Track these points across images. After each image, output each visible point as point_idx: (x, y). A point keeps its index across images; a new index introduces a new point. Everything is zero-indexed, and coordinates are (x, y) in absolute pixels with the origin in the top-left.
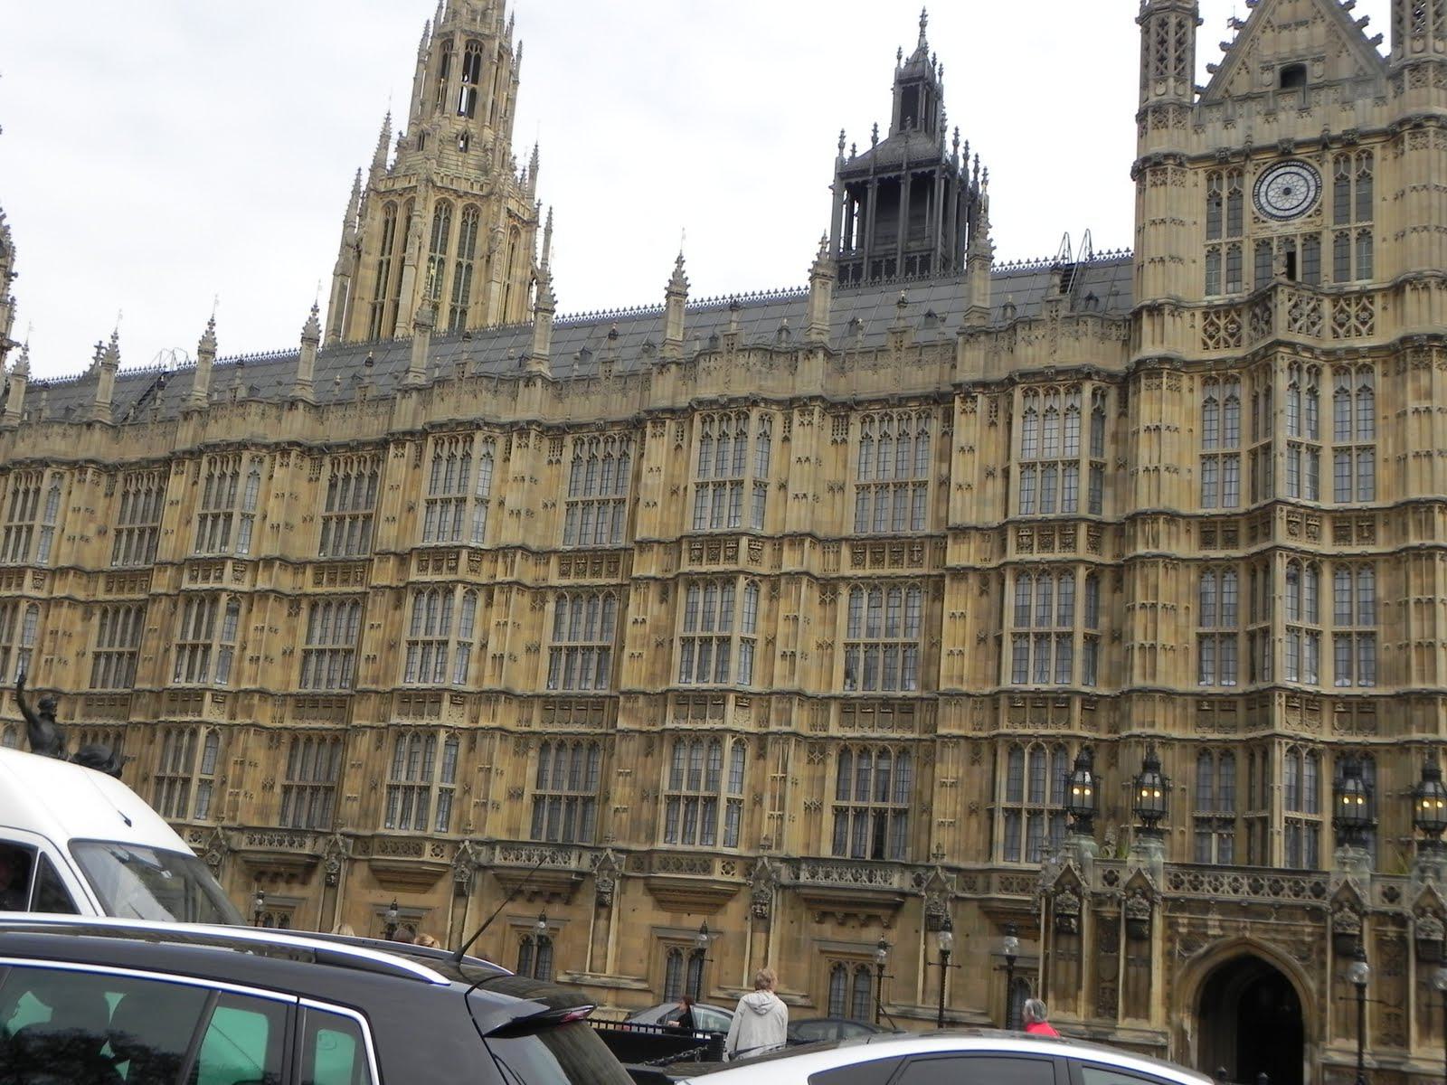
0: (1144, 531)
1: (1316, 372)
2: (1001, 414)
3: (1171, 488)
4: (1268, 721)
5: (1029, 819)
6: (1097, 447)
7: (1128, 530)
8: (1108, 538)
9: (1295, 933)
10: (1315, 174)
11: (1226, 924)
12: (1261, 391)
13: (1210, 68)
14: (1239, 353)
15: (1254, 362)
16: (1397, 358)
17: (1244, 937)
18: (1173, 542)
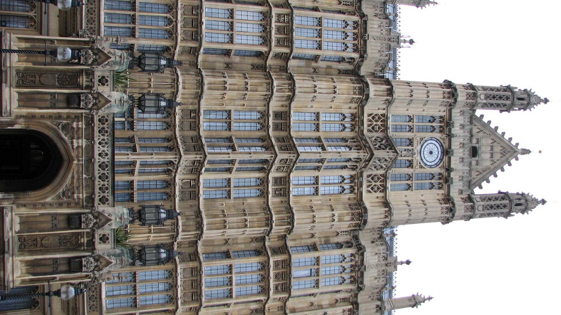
1: (354, 168)
2: (345, 8)
3: (305, 98)
4: (187, 151)
7: (284, 75)
8: (279, 62)
9: (78, 188)
10: (437, 165)
11: (80, 150)
12: (348, 143)
13: (482, 116)
14: (365, 132)
15: (362, 139)
16: (356, 205)
17: (73, 160)
18: (278, 99)
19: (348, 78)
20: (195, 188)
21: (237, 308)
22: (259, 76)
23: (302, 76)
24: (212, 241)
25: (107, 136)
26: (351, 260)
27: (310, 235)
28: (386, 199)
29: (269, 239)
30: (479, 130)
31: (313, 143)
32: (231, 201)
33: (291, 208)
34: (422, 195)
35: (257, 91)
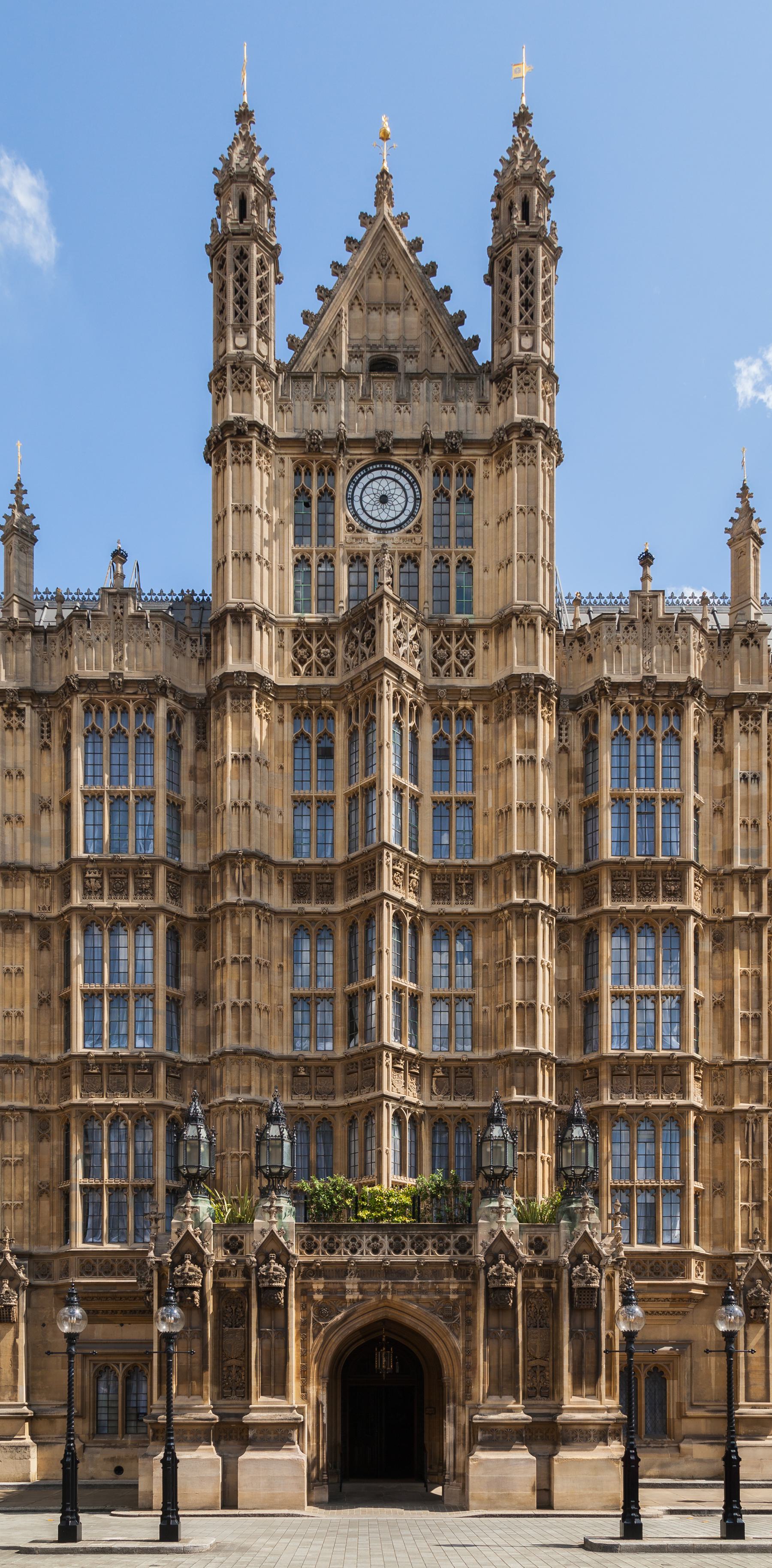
0: (234, 878)
3: (261, 830)
6: (174, 782)
14: (334, 681)
18: (265, 892)
19: (215, 726)
20: (449, 1068)
21: (707, 980)
22: (219, 934)
24: (559, 1032)
26: (628, 714)
27: (563, 818)
29: (564, 910)
30: (329, 349)
32: (479, 992)
33: (501, 861)
34: (486, 524)
35: (250, 939)
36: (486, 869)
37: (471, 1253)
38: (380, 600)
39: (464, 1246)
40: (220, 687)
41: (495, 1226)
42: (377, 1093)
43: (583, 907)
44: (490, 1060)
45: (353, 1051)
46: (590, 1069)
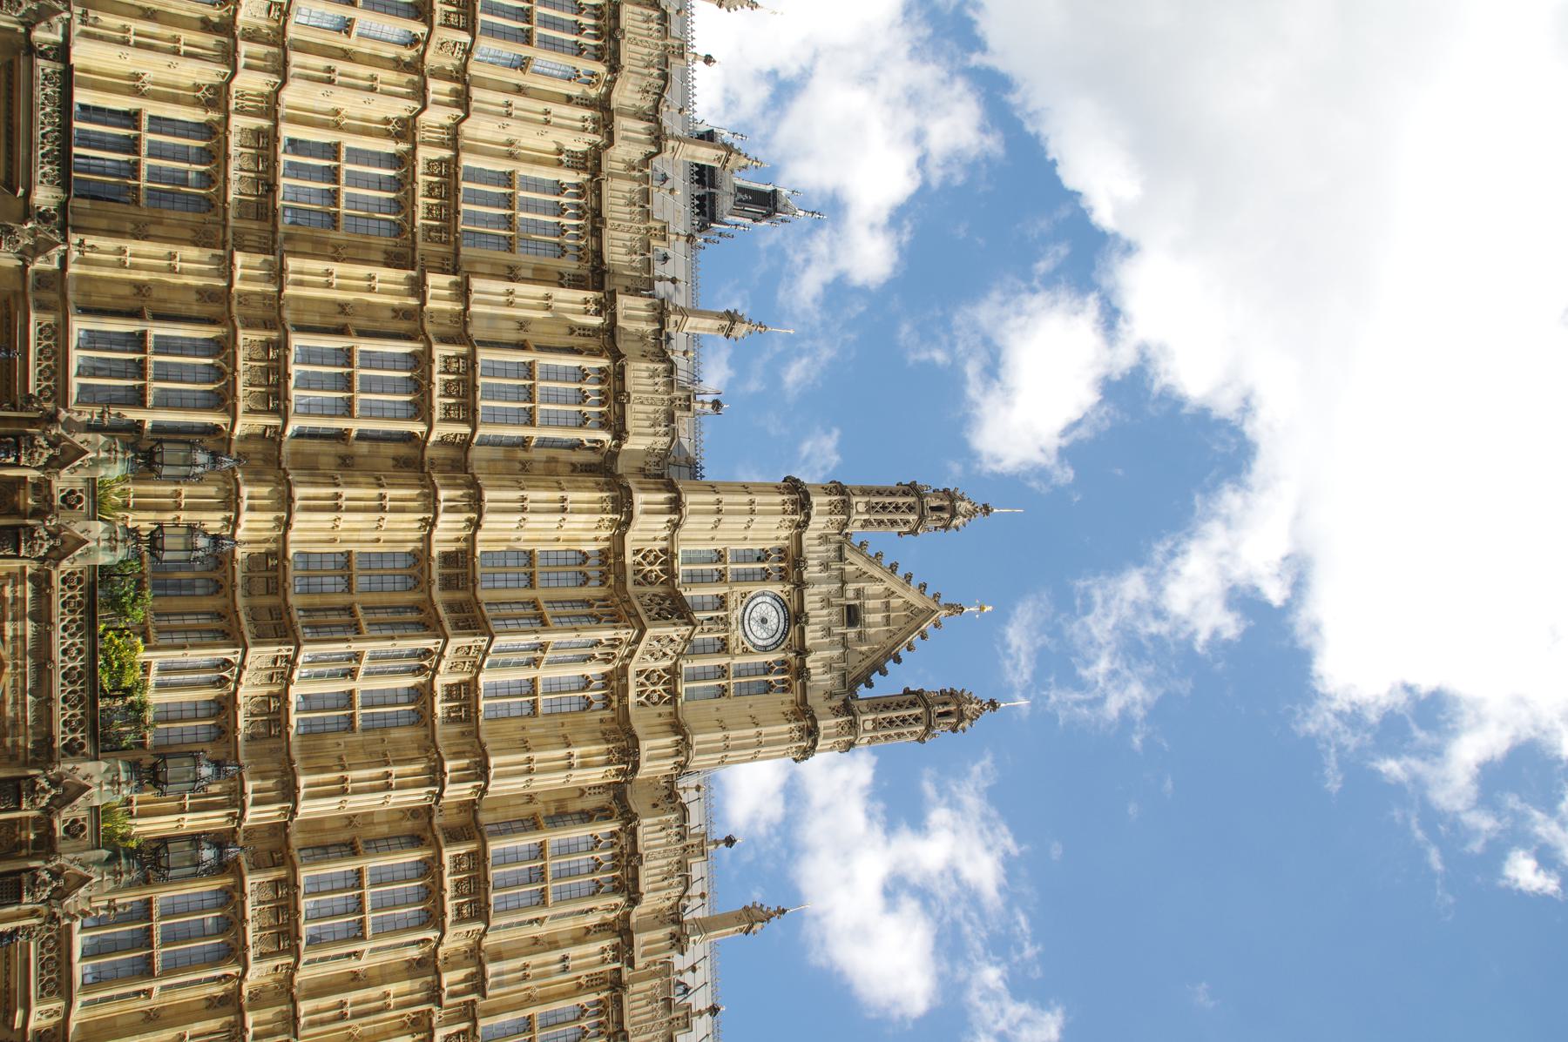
5: (133, 360)
7: (461, 478)
10: (777, 645)
12: (594, 610)
19: (590, 481)
23: (498, 479)
24: (321, 821)
25: (81, 613)
26: (612, 845)
27: (525, 799)
28: (677, 717)
31: (522, 611)
33: (482, 746)
36: (476, 733)
37: (63, 756)
38: (691, 622)
39: (71, 749)
40: (621, 487)
41: (96, 780)
42: (248, 640)
43: (444, 829)
44: (288, 754)
45: (295, 614)
46: (283, 858)
